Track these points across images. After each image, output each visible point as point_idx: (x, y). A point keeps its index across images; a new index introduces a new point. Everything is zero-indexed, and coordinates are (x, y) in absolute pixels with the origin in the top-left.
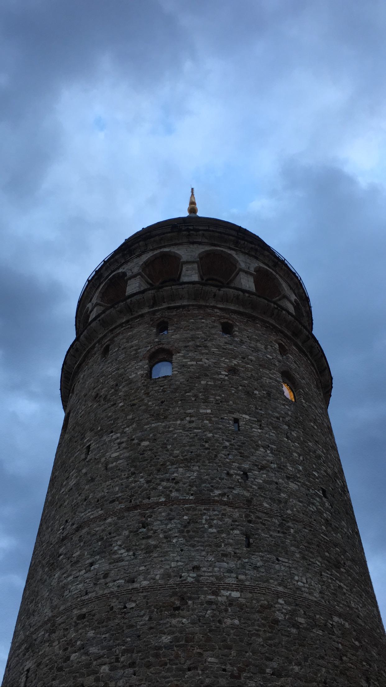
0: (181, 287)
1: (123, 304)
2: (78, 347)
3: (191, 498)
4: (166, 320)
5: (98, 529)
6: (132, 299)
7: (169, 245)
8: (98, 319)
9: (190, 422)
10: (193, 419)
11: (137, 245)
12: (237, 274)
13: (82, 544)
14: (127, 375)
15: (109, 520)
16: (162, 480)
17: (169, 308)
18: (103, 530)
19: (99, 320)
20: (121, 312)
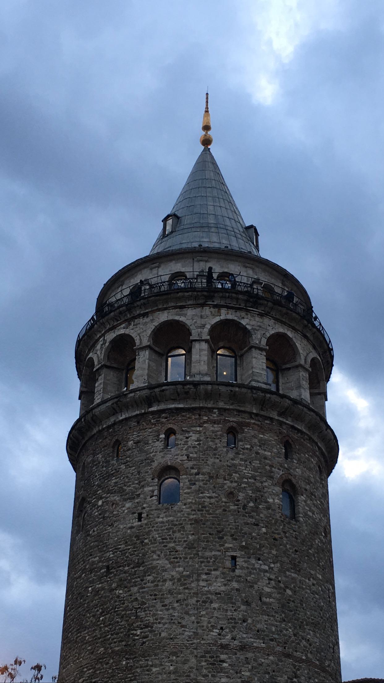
0: (309, 413)
1: (261, 394)
2: (191, 392)
3: (317, 662)
4: (290, 441)
5: (263, 661)
6: (272, 396)
7: (290, 325)
8: (230, 388)
9: (313, 585)
10: (315, 582)
11: (266, 302)
12: (320, 394)
13: (250, 667)
14: (266, 495)
15: (271, 658)
16: (303, 639)
17: (293, 427)
18: (268, 666)
19: (231, 391)
20: (255, 399)
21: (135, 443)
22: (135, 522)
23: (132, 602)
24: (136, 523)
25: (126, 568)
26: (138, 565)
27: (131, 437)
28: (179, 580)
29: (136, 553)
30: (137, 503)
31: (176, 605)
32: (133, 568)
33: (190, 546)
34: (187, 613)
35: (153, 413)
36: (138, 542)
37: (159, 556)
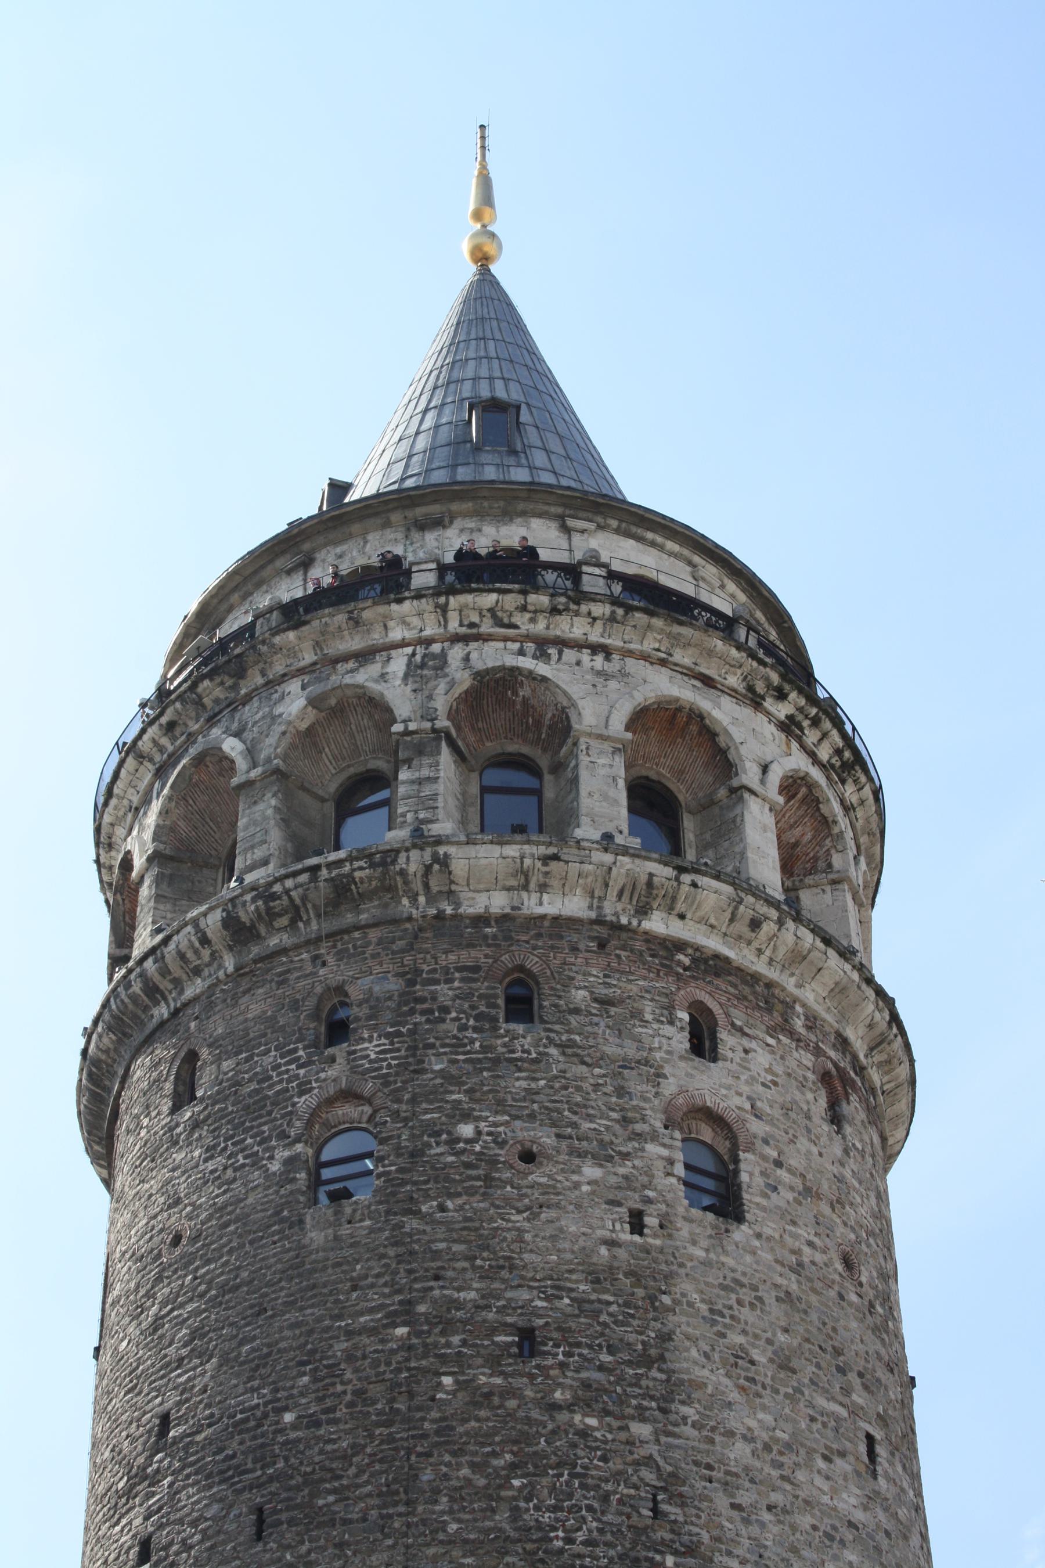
21: (596, 1000)
22: (623, 1230)
23: (637, 1463)
24: (626, 1236)
25: (606, 1358)
26: (646, 1361)
27: (580, 977)
28: (767, 1448)
29: (635, 1323)
30: (626, 1177)
31: (767, 1517)
32: (629, 1364)
33: (784, 1364)
34: (794, 1550)
35: (649, 938)
36: (640, 1292)
37: (706, 1355)
